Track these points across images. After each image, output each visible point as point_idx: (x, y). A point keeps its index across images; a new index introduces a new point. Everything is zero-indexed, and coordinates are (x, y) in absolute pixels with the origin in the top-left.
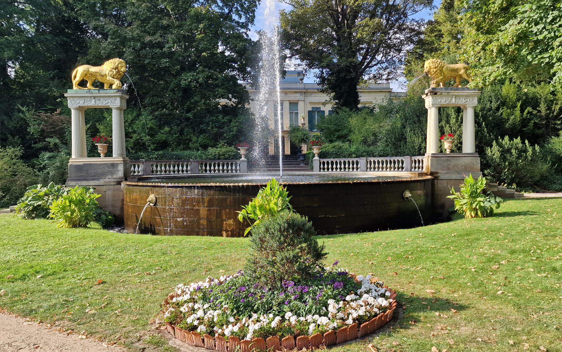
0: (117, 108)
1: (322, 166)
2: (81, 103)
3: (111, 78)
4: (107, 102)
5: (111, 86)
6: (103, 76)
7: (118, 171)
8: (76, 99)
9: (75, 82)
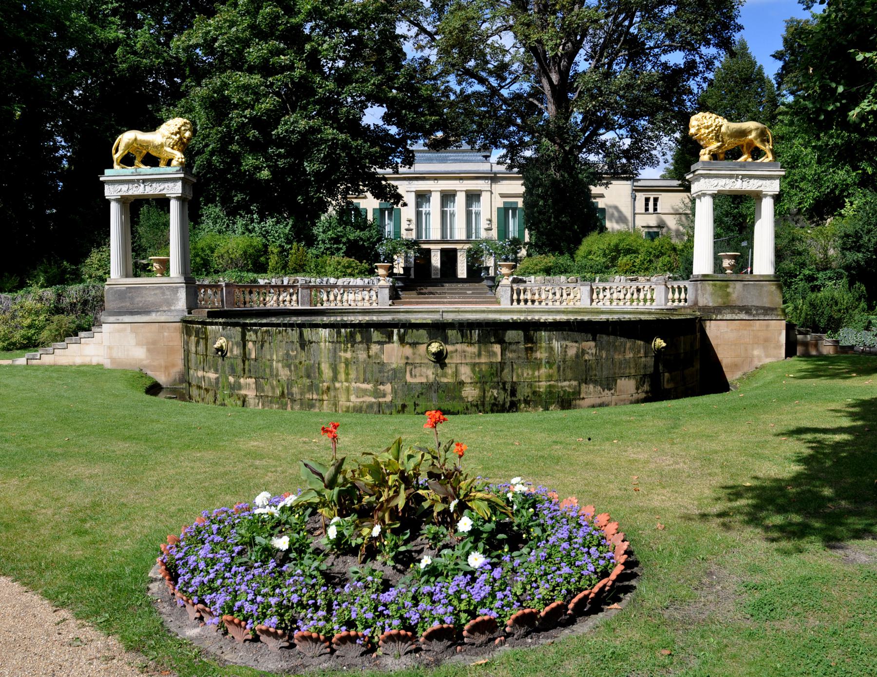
0: (177, 198)
1: (515, 297)
2: (125, 190)
3: (169, 150)
4: (162, 187)
5: (169, 163)
6: (156, 147)
7: (178, 300)
8: (119, 184)
9: (116, 157)
